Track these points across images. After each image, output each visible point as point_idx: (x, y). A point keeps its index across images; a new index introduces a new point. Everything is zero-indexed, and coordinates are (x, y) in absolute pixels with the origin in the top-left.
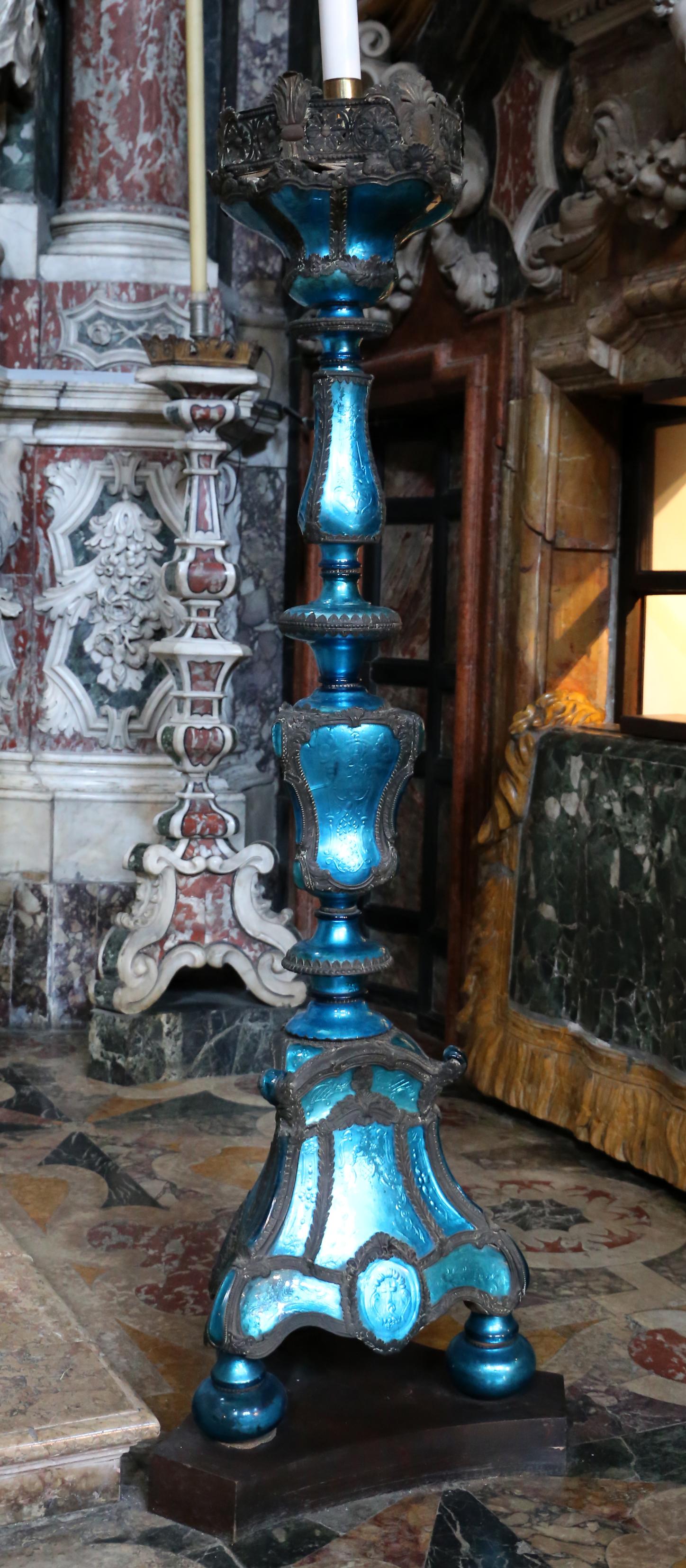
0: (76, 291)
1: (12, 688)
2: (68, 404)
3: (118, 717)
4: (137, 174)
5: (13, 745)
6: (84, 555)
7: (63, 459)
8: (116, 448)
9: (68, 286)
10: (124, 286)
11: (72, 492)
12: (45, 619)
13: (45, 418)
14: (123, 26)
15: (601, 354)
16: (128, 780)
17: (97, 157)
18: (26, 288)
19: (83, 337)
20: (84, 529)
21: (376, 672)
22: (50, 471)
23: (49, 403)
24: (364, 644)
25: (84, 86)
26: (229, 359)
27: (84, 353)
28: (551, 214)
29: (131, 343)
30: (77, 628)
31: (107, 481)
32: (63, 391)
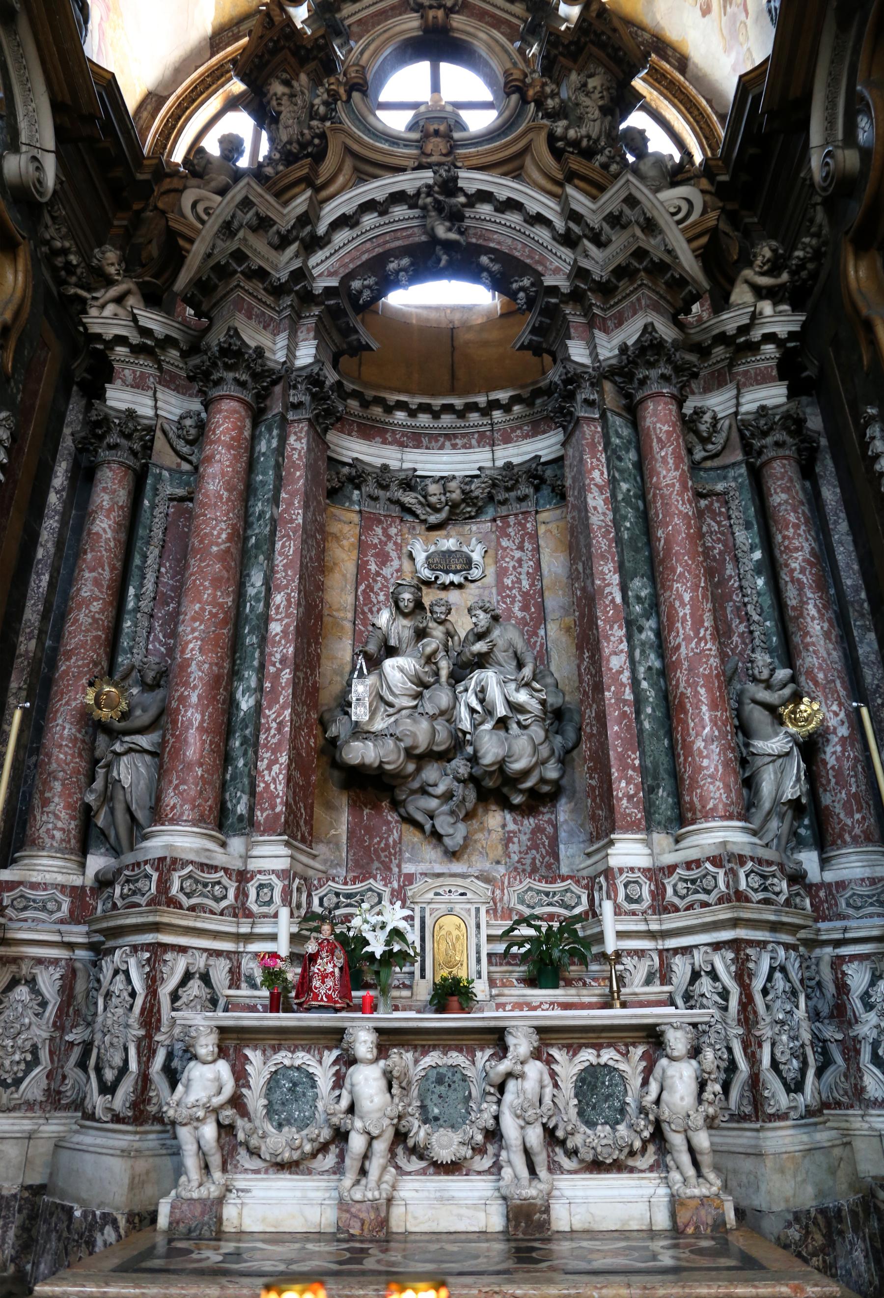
0: (841, 885)
1: (846, 1076)
2: (848, 935)
4: (857, 831)
5: (852, 1107)
6: (869, 1007)
7: (850, 961)
8: (875, 954)
9: (837, 883)
10: (863, 880)
12: (856, 1040)
13: (838, 943)
14: (839, 773)
17: (838, 827)
19: (848, 905)
22: (844, 968)
23: (840, 936)
25: (826, 799)
27: (851, 911)
29: (872, 904)
30: (873, 1044)
31: (873, 971)
32: (845, 930)
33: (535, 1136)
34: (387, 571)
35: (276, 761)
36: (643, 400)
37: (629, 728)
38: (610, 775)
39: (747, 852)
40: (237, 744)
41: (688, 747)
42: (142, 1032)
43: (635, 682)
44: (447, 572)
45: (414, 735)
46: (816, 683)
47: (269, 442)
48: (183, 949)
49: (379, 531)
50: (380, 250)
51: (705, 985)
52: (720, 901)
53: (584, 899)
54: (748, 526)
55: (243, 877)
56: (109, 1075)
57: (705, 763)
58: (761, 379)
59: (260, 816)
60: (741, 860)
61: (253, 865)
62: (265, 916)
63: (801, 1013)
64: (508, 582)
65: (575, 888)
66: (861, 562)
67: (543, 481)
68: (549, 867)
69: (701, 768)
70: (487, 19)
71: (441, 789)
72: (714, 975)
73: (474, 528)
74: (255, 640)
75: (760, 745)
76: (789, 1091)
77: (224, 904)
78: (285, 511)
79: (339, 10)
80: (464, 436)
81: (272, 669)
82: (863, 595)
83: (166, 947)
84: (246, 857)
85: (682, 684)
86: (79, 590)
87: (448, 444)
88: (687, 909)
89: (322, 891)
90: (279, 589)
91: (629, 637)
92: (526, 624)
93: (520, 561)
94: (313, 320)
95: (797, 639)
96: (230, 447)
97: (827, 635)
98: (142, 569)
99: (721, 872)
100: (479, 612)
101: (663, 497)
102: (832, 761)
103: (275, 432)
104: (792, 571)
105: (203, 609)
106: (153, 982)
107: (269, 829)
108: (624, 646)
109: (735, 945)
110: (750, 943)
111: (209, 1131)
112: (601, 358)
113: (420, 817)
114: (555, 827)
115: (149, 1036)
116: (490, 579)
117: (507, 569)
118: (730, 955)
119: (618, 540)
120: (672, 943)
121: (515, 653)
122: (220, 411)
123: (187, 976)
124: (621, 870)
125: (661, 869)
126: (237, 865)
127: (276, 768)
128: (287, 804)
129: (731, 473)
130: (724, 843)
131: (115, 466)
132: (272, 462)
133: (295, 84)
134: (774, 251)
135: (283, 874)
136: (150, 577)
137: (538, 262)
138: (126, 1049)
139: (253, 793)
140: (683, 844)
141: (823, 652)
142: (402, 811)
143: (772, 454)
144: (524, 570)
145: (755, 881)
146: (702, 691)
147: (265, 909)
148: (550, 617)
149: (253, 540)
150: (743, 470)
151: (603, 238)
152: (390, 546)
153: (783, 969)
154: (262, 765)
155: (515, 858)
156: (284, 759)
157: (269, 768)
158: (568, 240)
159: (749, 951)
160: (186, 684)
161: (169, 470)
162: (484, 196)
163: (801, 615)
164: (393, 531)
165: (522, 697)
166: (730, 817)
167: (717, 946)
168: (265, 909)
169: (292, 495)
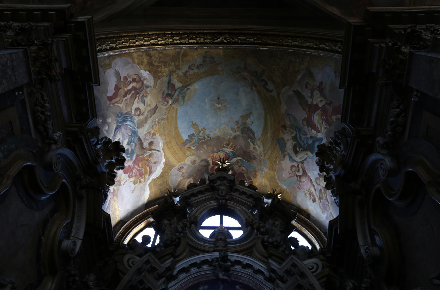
50: (197, 282)
133: (172, 221)
158: (270, 280)
162: (238, 262)
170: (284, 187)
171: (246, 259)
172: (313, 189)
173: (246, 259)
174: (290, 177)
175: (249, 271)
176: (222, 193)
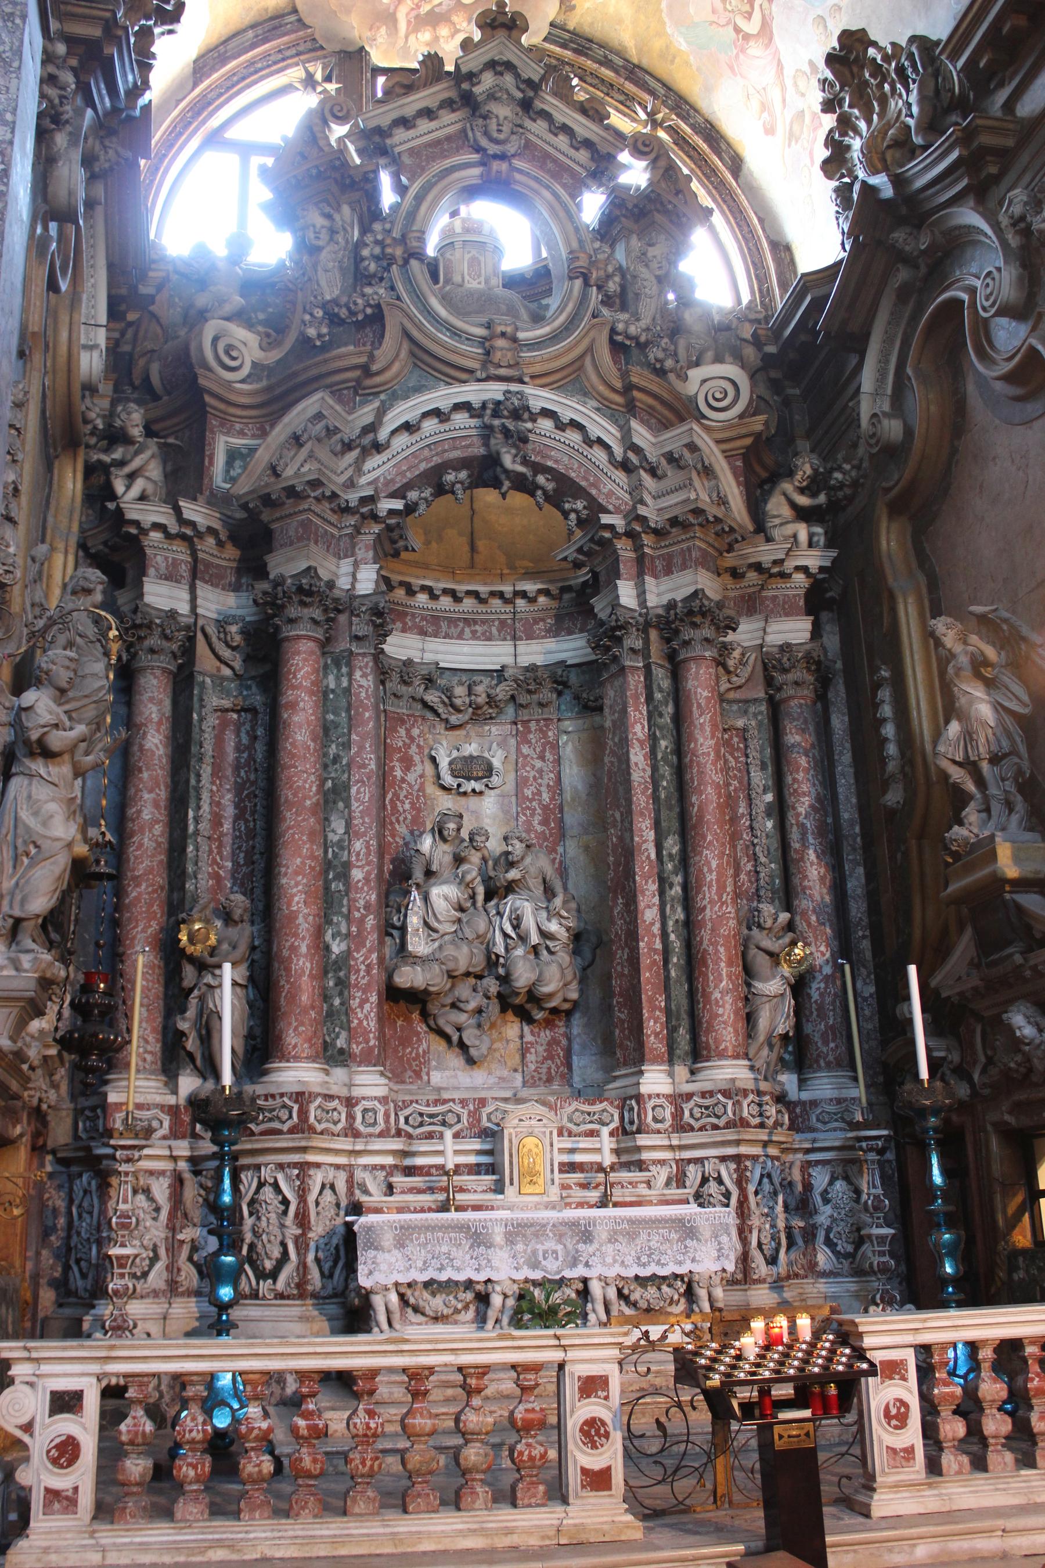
0: (814, 1103)
3: (846, 1263)
4: (831, 1058)
6: (826, 1201)
11: (820, 1178)
12: (814, 1227)
13: (808, 1151)
14: (820, 1008)
15: (1007, 1117)
16: (853, 1287)
18: (796, 1104)
20: (826, 1191)
21: (951, 1222)
24: (946, 1214)
25: (808, 1029)
26: (878, 1127)
27: (819, 1125)
28: (984, 1071)
32: (814, 1141)
33: (612, 1293)
34: (411, 777)
35: (367, 1000)
36: (684, 661)
37: (658, 973)
38: (641, 1015)
39: (750, 1085)
40: (331, 983)
41: (706, 996)
42: (299, 1231)
43: (664, 935)
44: (469, 779)
45: (456, 959)
46: (809, 925)
47: (338, 679)
48: (318, 1165)
49: (402, 732)
50: (437, 460)
51: (712, 1187)
52: (728, 1125)
53: (616, 1117)
54: (763, 767)
55: (350, 1102)
56: (268, 1265)
57: (721, 1011)
58: (788, 611)
59: (356, 1049)
60: (745, 1093)
61: (357, 1092)
62: (371, 1135)
63: (779, 1208)
64: (528, 793)
65: (610, 1109)
66: (859, 796)
67: (565, 684)
68: (563, 1076)
69: (717, 1015)
70: (550, 165)
71: (472, 1005)
72: (720, 1181)
73: (494, 729)
74: (341, 887)
75: (759, 986)
76: (768, 1263)
77: (340, 1126)
78: (358, 754)
79: (390, 136)
80: (484, 622)
81: (357, 915)
82: (857, 829)
83: (310, 1165)
84: (350, 1085)
85: (706, 942)
86: (139, 812)
87: (467, 630)
88: (701, 1129)
89: (407, 1112)
90: (358, 835)
91: (662, 893)
92: (546, 839)
93: (540, 771)
94: (372, 537)
95: (796, 881)
96: (312, 693)
97: (822, 879)
98: (198, 789)
99: (730, 1103)
100: (516, 842)
101: (699, 764)
102: (815, 996)
103: (344, 670)
104: (798, 815)
105: (303, 863)
106: (302, 1193)
107: (367, 1059)
108: (656, 900)
109: (737, 1158)
110: (747, 1157)
111: (394, 1298)
112: (649, 604)
113: (449, 1030)
114: (569, 1040)
115: (304, 1234)
116: (510, 787)
117: (527, 779)
118: (733, 1166)
119: (655, 798)
120: (687, 1155)
121: (544, 881)
122: (299, 653)
123: (323, 1186)
124: (650, 1096)
125: (680, 1095)
126: (344, 1092)
127: (367, 1006)
128: (378, 1039)
129: (752, 709)
130: (733, 1080)
131: (158, 672)
132: (344, 703)
133: (337, 217)
134: (815, 471)
135: (384, 1100)
136: (205, 796)
137: (593, 485)
138: (284, 1245)
139: (349, 1029)
140: (701, 1076)
141: (817, 897)
142: (432, 1023)
143: (791, 692)
144: (545, 782)
145: (755, 1109)
146: (722, 949)
147: (370, 1130)
148: (569, 833)
149: (329, 784)
150: (763, 708)
151: (659, 472)
152: (414, 749)
153: (769, 1176)
154: (354, 1003)
155: (532, 1067)
156: (374, 998)
157: (361, 1006)
159: (748, 1163)
160: (296, 935)
161: (211, 676)
162: (547, 413)
163: (802, 859)
164: (415, 732)
165: (553, 927)
166: (736, 1057)
167: (723, 1159)
168: (370, 1130)
169: (363, 737)
170: (681, 44)
171: (570, 407)
172: (775, 94)
173: (570, 407)
174: (712, 23)
175: (574, 437)
176: (499, 131)
